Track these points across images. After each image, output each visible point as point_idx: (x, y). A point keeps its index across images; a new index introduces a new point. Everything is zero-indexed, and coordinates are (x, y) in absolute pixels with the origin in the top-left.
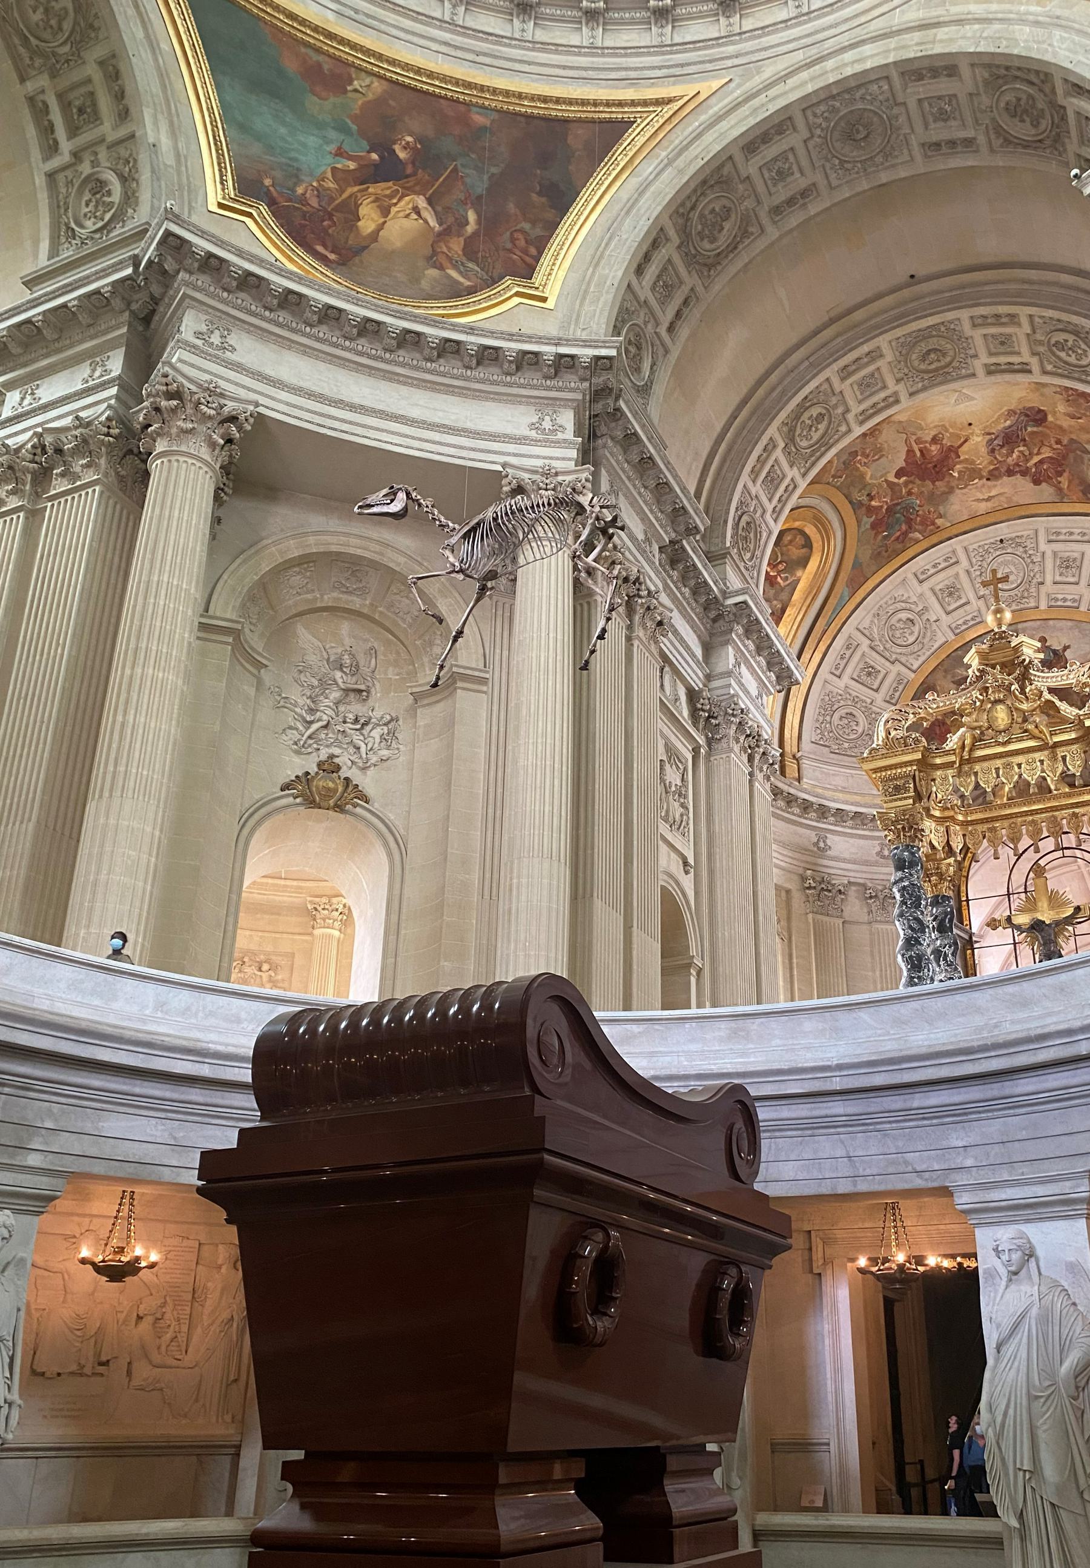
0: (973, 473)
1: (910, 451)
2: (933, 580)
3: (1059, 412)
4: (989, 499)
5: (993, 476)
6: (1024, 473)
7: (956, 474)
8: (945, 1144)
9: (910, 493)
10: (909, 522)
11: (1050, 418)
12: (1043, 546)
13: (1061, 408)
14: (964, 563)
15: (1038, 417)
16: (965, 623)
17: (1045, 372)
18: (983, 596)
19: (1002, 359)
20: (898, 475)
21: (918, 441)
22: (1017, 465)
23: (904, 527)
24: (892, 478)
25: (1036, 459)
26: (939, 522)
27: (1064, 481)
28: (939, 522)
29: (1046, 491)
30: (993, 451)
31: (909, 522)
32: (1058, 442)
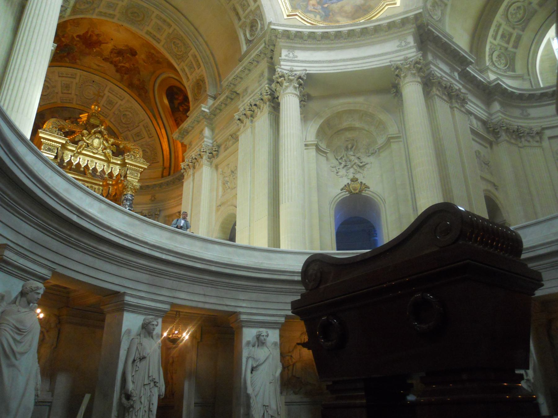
0: (100, 54)
1: (87, 32)
2: (63, 79)
3: (141, 56)
4: (98, 66)
5: (106, 60)
6: (116, 66)
7: (95, 50)
8: (237, 298)
9: (76, 45)
10: (68, 54)
11: (137, 56)
12: (106, 92)
13: (143, 56)
14: (77, 80)
15: (133, 53)
16: (66, 100)
17: (163, 46)
18: (76, 95)
19: (155, 33)
20: (78, 36)
21: (93, 32)
22: (115, 62)
23: (65, 54)
24: (75, 35)
25: (123, 65)
26: (77, 61)
27: (126, 77)
28: (77, 61)
29: (118, 76)
30: (111, 52)
31: (68, 54)
32: (133, 65)
